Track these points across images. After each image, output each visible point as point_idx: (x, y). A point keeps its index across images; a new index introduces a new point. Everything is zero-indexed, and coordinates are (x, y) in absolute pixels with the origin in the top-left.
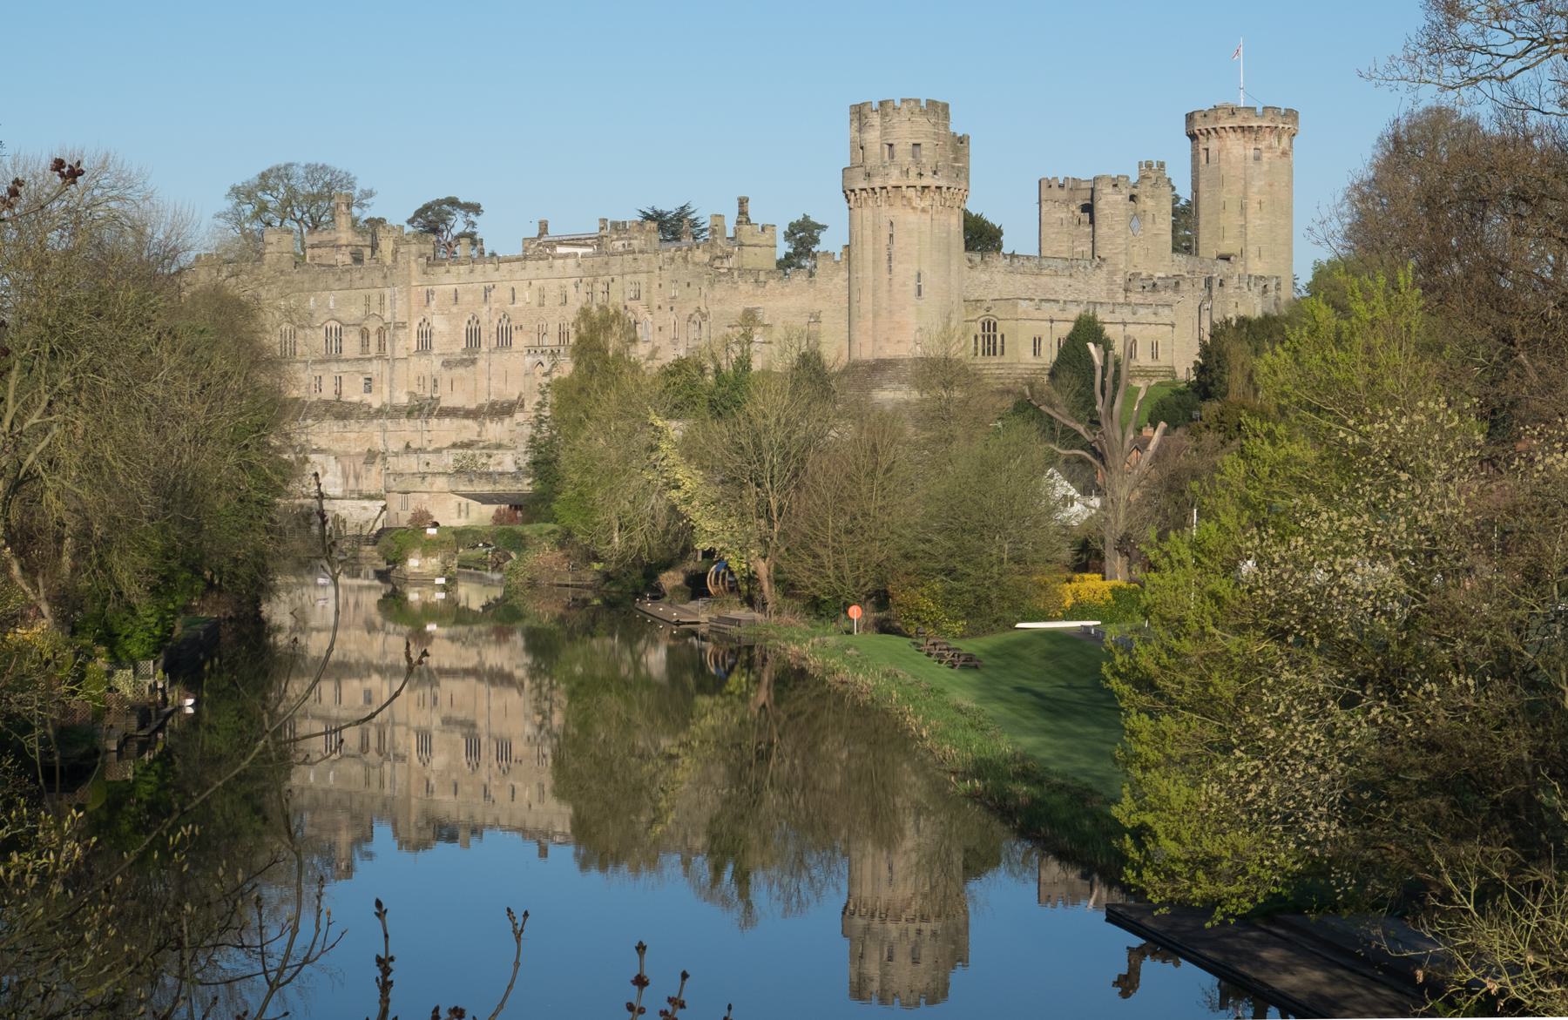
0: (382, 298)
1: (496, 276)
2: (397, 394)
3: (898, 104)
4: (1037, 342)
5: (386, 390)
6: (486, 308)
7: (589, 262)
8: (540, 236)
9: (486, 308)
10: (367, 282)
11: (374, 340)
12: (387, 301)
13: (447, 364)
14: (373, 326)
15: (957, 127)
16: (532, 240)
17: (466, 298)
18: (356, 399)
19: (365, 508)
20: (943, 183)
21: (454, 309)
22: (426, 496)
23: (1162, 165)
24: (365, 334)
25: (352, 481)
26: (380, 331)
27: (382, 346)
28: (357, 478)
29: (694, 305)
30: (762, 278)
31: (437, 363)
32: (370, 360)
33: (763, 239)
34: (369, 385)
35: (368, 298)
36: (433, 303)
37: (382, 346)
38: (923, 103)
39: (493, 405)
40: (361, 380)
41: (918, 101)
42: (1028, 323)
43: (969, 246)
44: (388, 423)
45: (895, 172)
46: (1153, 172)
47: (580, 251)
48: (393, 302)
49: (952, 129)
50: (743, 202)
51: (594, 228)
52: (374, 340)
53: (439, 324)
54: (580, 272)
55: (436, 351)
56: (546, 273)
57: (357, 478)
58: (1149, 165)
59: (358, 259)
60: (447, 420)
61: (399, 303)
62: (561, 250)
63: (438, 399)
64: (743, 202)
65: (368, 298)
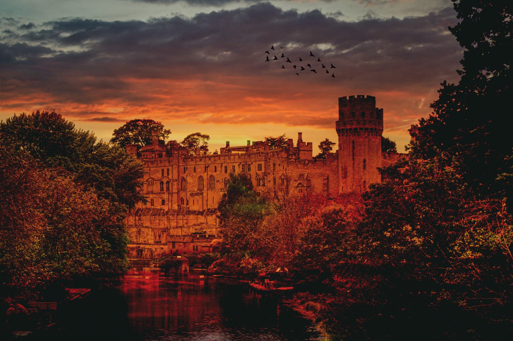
0: (168, 170)
1: (209, 162)
2: (174, 206)
5: (170, 204)
6: (206, 174)
7: (243, 157)
8: (227, 147)
9: (206, 174)
10: (163, 164)
11: (165, 186)
12: (170, 172)
13: (192, 195)
14: (165, 180)
15: (378, 106)
16: (224, 149)
17: (198, 170)
18: (159, 207)
19: (162, 248)
20: (373, 127)
21: (194, 174)
22: (182, 244)
24: (162, 183)
25: (157, 238)
26: (168, 182)
27: (168, 189)
28: (160, 236)
29: (281, 172)
30: (306, 162)
31: (188, 194)
32: (164, 193)
33: (308, 148)
34: (163, 203)
35: (163, 170)
36: (186, 172)
37: (168, 189)
38: (365, 97)
39: (208, 210)
40: (161, 200)
41: (363, 96)
43: (384, 150)
44: (171, 216)
47: (240, 153)
48: (172, 172)
50: (300, 134)
51: (246, 144)
52: (165, 186)
53: (189, 180)
54: (240, 161)
55: (188, 190)
56: (228, 161)
57: (160, 236)
59: (160, 156)
60: (192, 216)
61: (174, 172)
62: (233, 152)
63: (189, 208)
64: (300, 134)
65: (163, 170)
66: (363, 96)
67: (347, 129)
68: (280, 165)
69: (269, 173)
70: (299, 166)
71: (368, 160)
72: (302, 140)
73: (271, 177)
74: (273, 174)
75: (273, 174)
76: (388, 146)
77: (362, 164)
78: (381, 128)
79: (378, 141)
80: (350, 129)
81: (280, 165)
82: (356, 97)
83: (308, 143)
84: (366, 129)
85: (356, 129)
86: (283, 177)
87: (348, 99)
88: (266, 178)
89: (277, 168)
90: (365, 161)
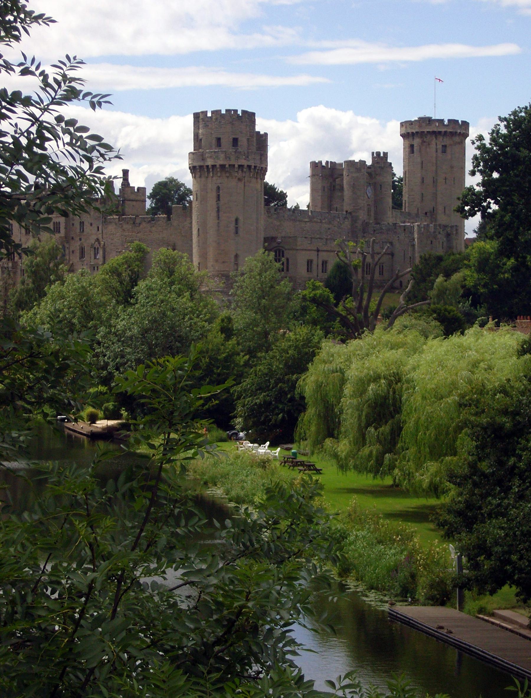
3: (223, 112)
4: (310, 263)
20: (252, 163)
23: (386, 154)
29: (95, 237)
38: (240, 113)
41: (237, 111)
42: (304, 252)
45: (222, 156)
46: (381, 160)
49: (257, 129)
50: (126, 173)
58: (378, 154)
64: (126, 173)
66: (237, 111)
67: (207, 166)
68: (91, 225)
69: (73, 238)
70: (125, 226)
71: (241, 219)
72: (129, 184)
73: (75, 245)
74: (80, 239)
75: (80, 239)
76: (274, 197)
77: (232, 226)
78: (263, 166)
79: (258, 186)
80: (214, 166)
81: (91, 225)
82: (223, 112)
83: (139, 189)
84: (241, 167)
85: (223, 167)
86: (96, 245)
87: (209, 115)
88: (67, 245)
89: (87, 228)
90: (237, 220)
